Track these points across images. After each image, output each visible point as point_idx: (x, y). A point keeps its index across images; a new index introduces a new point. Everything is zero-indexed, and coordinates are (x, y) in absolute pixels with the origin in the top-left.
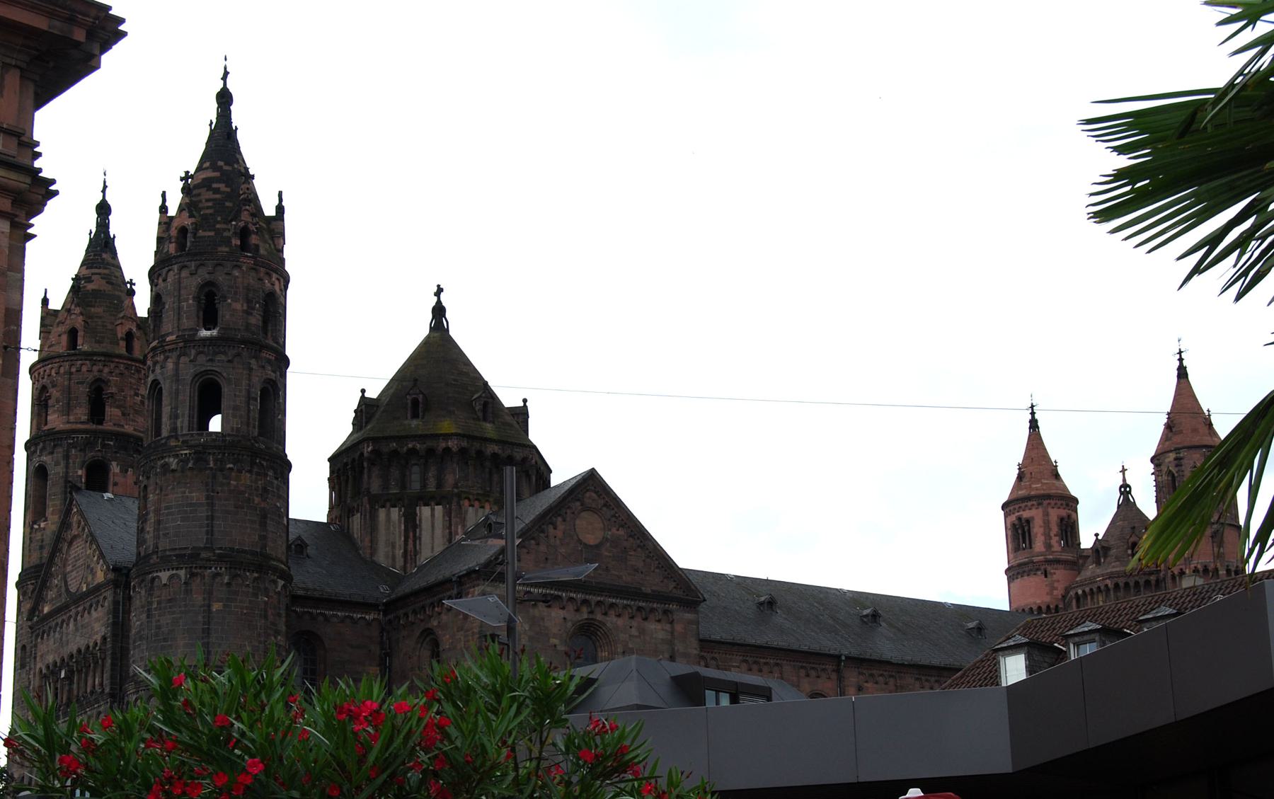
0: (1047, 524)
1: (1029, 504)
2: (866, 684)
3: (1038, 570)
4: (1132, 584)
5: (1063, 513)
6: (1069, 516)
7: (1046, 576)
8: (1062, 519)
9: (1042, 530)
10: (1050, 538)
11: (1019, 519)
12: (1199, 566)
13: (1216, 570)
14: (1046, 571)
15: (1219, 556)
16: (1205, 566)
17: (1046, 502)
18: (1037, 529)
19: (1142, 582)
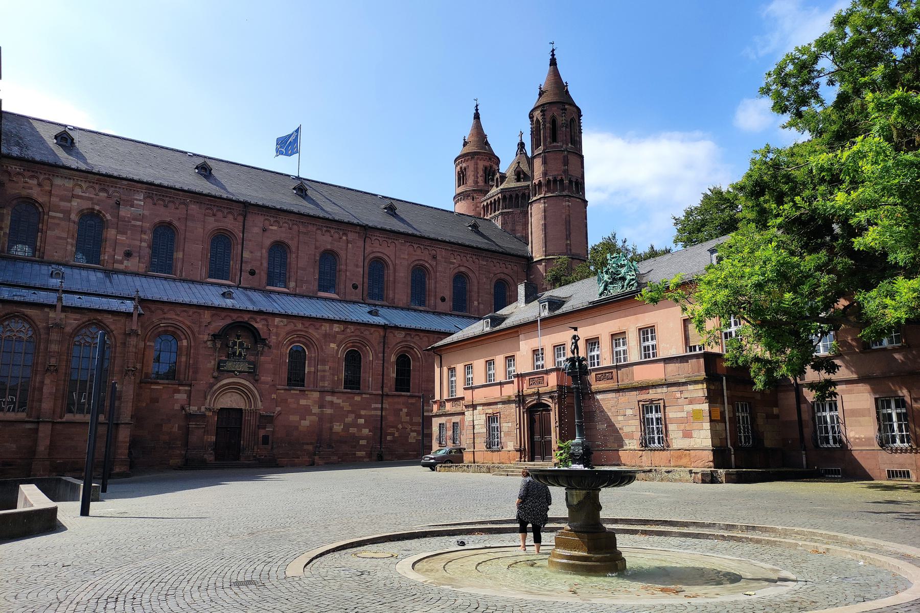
0: (476, 169)
1: (467, 158)
2: (271, 227)
3: (468, 197)
4: (514, 196)
5: (487, 164)
6: (491, 167)
7: (473, 200)
8: (486, 168)
9: (473, 173)
10: (477, 178)
11: (461, 168)
12: (551, 178)
13: (562, 180)
14: (473, 197)
15: (566, 172)
16: (555, 178)
17: (476, 157)
18: (470, 174)
19: (520, 194)
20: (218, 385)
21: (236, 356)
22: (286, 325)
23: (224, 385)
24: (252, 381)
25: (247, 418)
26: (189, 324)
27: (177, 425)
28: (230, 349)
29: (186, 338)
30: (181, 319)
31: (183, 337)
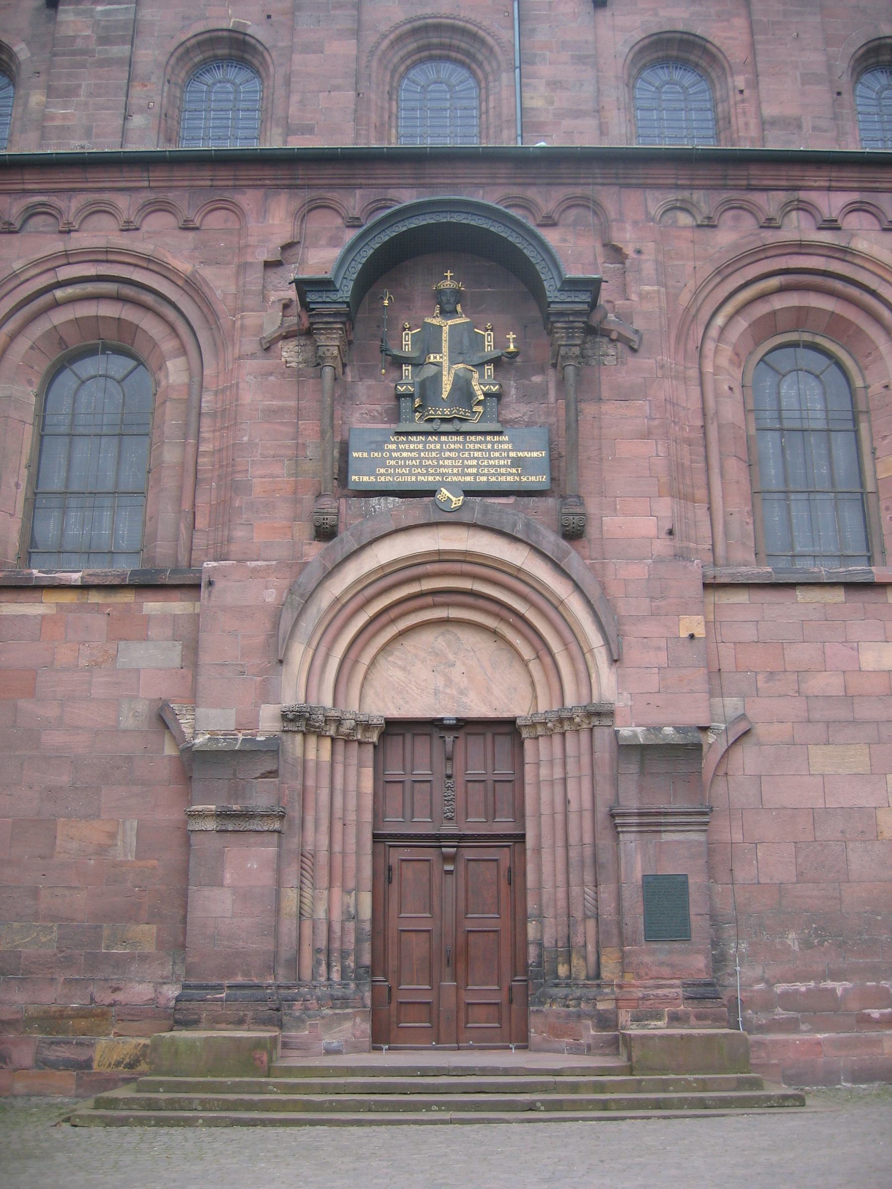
20: (352, 573)
21: (439, 402)
22: (710, 225)
23: (384, 572)
24: (550, 540)
25: (544, 772)
26: (184, 266)
27: (133, 824)
28: (407, 370)
29: (183, 351)
30: (145, 247)
31: (168, 345)
